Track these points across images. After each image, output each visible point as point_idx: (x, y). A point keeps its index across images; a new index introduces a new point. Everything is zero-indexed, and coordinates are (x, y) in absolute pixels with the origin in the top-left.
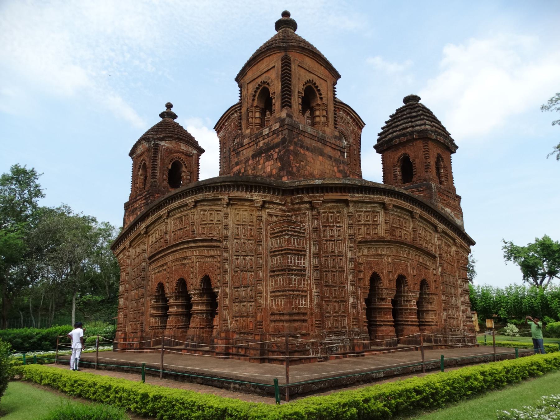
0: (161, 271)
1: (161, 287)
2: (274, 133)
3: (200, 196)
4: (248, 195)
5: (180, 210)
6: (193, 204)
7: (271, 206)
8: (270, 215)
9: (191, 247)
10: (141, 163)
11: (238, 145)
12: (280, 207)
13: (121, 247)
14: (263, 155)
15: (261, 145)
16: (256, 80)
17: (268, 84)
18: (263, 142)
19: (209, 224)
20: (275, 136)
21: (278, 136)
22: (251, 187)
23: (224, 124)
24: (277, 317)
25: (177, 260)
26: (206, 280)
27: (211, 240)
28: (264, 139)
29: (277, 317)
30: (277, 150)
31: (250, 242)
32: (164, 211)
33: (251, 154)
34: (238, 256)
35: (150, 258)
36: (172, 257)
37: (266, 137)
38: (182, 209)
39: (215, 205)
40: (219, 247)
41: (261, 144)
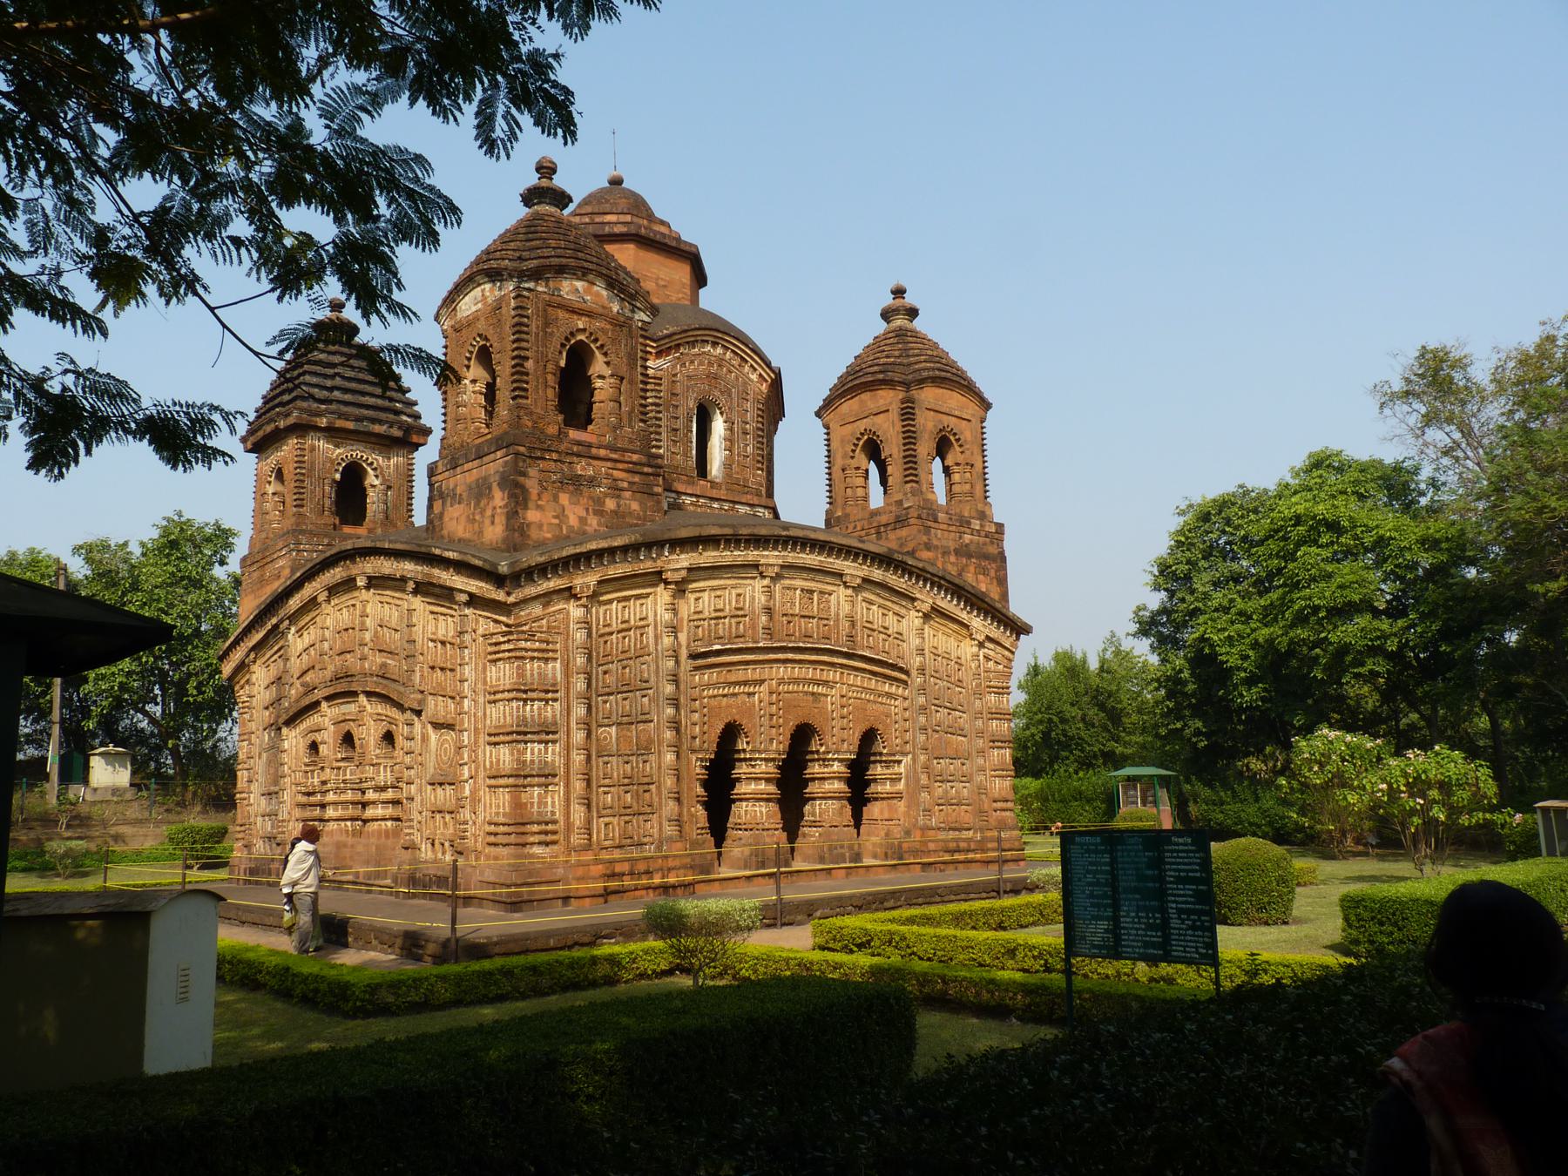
0: (734, 695)
1: (731, 732)
3: (877, 574)
4: (964, 616)
6: (859, 581)
7: (991, 646)
8: (987, 658)
9: (842, 666)
10: (572, 334)
24: (999, 805)
25: (796, 681)
26: (869, 737)
27: (894, 667)
29: (999, 805)
32: (771, 557)
33: (952, 545)
35: (694, 656)
36: (782, 671)
40: (905, 683)
41: (967, 538)
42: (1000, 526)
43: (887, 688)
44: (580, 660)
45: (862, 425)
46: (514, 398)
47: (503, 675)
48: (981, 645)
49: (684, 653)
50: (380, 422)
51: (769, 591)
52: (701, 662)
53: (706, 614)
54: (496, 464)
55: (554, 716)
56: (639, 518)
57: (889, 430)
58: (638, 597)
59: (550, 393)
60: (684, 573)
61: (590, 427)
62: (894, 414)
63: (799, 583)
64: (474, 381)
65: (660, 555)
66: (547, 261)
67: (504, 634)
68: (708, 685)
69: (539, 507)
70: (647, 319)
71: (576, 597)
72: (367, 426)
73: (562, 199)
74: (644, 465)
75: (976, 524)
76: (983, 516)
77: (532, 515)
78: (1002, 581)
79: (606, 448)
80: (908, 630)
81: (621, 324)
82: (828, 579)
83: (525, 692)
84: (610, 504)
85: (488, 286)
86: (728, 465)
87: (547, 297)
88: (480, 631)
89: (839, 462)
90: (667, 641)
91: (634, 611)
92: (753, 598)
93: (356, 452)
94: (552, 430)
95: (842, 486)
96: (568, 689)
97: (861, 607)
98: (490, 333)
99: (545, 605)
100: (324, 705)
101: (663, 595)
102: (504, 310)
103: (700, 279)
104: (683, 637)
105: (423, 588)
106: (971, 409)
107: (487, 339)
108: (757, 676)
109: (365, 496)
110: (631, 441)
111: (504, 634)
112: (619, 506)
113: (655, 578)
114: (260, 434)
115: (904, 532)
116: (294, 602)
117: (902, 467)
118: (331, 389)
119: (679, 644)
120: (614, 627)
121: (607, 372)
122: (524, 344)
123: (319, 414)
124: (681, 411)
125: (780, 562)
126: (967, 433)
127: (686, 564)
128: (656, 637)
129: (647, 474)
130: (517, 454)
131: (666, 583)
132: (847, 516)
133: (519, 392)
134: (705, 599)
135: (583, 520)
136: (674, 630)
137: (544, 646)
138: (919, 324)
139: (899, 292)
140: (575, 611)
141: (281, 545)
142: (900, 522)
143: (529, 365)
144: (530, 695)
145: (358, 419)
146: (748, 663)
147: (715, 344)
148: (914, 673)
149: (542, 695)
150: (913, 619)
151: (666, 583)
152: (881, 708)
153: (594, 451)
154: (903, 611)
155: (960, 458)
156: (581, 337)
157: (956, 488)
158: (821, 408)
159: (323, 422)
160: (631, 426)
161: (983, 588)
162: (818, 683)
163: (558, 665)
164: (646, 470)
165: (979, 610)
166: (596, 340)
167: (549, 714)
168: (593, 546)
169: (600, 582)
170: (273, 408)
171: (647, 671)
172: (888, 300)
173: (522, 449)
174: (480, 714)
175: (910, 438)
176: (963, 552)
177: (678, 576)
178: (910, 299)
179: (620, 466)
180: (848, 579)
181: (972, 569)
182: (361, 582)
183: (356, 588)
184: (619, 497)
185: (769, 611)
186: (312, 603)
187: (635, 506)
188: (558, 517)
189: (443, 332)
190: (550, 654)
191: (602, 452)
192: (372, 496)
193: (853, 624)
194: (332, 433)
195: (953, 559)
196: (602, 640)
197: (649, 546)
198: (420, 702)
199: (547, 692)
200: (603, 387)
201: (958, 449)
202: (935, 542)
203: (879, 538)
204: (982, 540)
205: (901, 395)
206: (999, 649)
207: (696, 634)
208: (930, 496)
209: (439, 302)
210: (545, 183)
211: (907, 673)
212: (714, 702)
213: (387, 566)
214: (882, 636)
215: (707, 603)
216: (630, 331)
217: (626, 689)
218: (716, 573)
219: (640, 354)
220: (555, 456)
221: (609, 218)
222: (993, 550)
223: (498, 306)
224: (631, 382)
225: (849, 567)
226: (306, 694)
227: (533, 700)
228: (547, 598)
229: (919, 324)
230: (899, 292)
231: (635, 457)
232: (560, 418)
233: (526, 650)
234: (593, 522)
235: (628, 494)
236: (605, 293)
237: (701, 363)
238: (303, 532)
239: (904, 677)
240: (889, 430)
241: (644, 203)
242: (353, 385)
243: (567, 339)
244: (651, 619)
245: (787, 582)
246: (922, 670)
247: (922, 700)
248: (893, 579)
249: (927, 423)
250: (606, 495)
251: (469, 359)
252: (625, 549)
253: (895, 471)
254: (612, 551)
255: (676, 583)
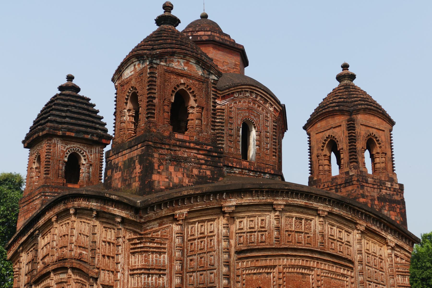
2: (395, 190)
3: (336, 210)
4: (383, 233)
5: (301, 210)
6: (326, 213)
7: (398, 250)
8: (396, 256)
9: (317, 259)
10: (178, 86)
11: (363, 179)
12: (407, 253)
13: (164, 212)
14: (387, 203)
15: (384, 193)
16: (368, 128)
17: (378, 141)
18: (385, 191)
19: (338, 241)
20: (395, 193)
21: (397, 195)
22: (388, 227)
23: (233, 93)
25: (293, 267)
28: (386, 190)
30: (399, 206)
31: (380, 272)
32: (280, 201)
34: (371, 282)
36: (285, 261)
37: (388, 189)
38: (305, 211)
39: (344, 225)
40: (352, 268)
41: (384, 192)
42: (401, 186)
43: (342, 271)
44: (178, 254)
45: (327, 134)
46: (147, 118)
47: (137, 261)
48: (393, 249)
49: (233, 250)
50: (88, 133)
51: (278, 218)
52: (242, 256)
53: (245, 230)
54: (136, 152)
55: (163, 283)
56: (210, 179)
57: (341, 135)
58: (209, 221)
59: (166, 115)
60: (233, 208)
61: (187, 132)
62: (344, 127)
63: (294, 214)
64: (129, 110)
65: (221, 198)
66: (166, 50)
67: (138, 239)
68: (246, 268)
69: (159, 173)
70: (216, 78)
71: (175, 220)
72: (82, 136)
73: (176, 21)
74: (213, 152)
75: (388, 185)
76: (392, 180)
77: (155, 177)
78: (403, 215)
79: (193, 143)
80: (353, 241)
81: (203, 81)
82: (310, 212)
83: (149, 269)
84: (195, 172)
85: (137, 63)
86: (257, 154)
87: (166, 68)
88: (127, 237)
89: (315, 152)
90: (224, 244)
91: (207, 228)
92: (270, 222)
93: (75, 146)
94: (166, 134)
95: (318, 164)
96: (171, 269)
97: (327, 227)
98: (137, 86)
99: (160, 225)
100: (52, 274)
101: (222, 221)
102: (144, 75)
103: (245, 63)
104: (232, 242)
105: (100, 215)
106: (385, 125)
107: (136, 89)
108: (272, 264)
109: (79, 169)
110: (207, 140)
111: (138, 239)
112: (199, 172)
113: (218, 211)
114: (31, 139)
115: (350, 188)
116: (41, 222)
117: (348, 155)
118: (65, 117)
119: (231, 246)
120: (196, 236)
121: (195, 105)
122: (153, 91)
123: (59, 130)
124: (234, 127)
125: (284, 203)
126: (382, 136)
127: (234, 203)
128: (218, 242)
129: (215, 157)
130: (148, 146)
131: (224, 213)
132: (320, 180)
133: (150, 114)
134: (245, 223)
135: (181, 180)
136: (227, 238)
137: (159, 246)
138: (356, 82)
139: (345, 67)
140: (176, 228)
141: (37, 193)
142: (348, 182)
143: (156, 101)
144: (151, 272)
145: (78, 132)
146: (267, 256)
147: (251, 92)
148: (356, 263)
149: (157, 272)
150: (355, 235)
151: (224, 213)
152: (339, 282)
153: (187, 144)
154: (350, 230)
155: (379, 150)
156: (182, 87)
157: (378, 166)
158: (306, 125)
159: (60, 133)
160: (207, 132)
161: (393, 218)
162: (305, 268)
163: (166, 256)
164: (214, 154)
165: (391, 229)
166: (190, 89)
167: (161, 282)
168: (185, 193)
169: (189, 212)
170: (37, 126)
171: (214, 259)
172: (340, 71)
173: (150, 143)
174: (126, 281)
175: (352, 140)
176: (381, 199)
177: (230, 210)
178: (351, 70)
179: (201, 152)
180: (320, 212)
181: (387, 208)
182: (72, 212)
183: (70, 215)
184: (200, 168)
185: (278, 229)
186: (49, 223)
187: (208, 173)
188: (168, 177)
189: (116, 87)
190: (162, 250)
191: (192, 145)
192: (83, 169)
193: (323, 236)
194: (65, 138)
195: (376, 202)
196: (190, 243)
197: (215, 193)
198: (97, 273)
199: (160, 270)
200: (193, 112)
201: (378, 145)
202: (367, 194)
203: (337, 191)
204: (392, 193)
205: (347, 118)
206: (402, 251)
207: (239, 240)
208: (364, 170)
209: (114, 72)
210: (167, 14)
211: (352, 262)
212: (249, 277)
213: (84, 204)
214: (339, 243)
215: (246, 224)
216: (208, 85)
217: (203, 269)
218: (251, 209)
219: (212, 96)
220: (167, 147)
221: (200, 33)
222: (397, 198)
223: (141, 73)
224: (207, 110)
225: (320, 206)
226: (44, 268)
227: (153, 274)
228: (161, 220)
229: (356, 82)
230: (345, 67)
231: (209, 148)
232: (171, 128)
233: (150, 247)
234: (186, 180)
235: (204, 167)
236: (195, 66)
237: (244, 102)
238: (48, 187)
239: (351, 265)
240: (341, 135)
241: (218, 26)
242: (75, 116)
243: (175, 88)
244: (216, 232)
245: (288, 214)
246: (361, 262)
247: (361, 278)
248: (343, 213)
249: (361, 132)
250: (194, 167)
251: (127, 99)
252: (202, 195)
253: (345, 156)
254: (195, 196)
255: (230, 213)
